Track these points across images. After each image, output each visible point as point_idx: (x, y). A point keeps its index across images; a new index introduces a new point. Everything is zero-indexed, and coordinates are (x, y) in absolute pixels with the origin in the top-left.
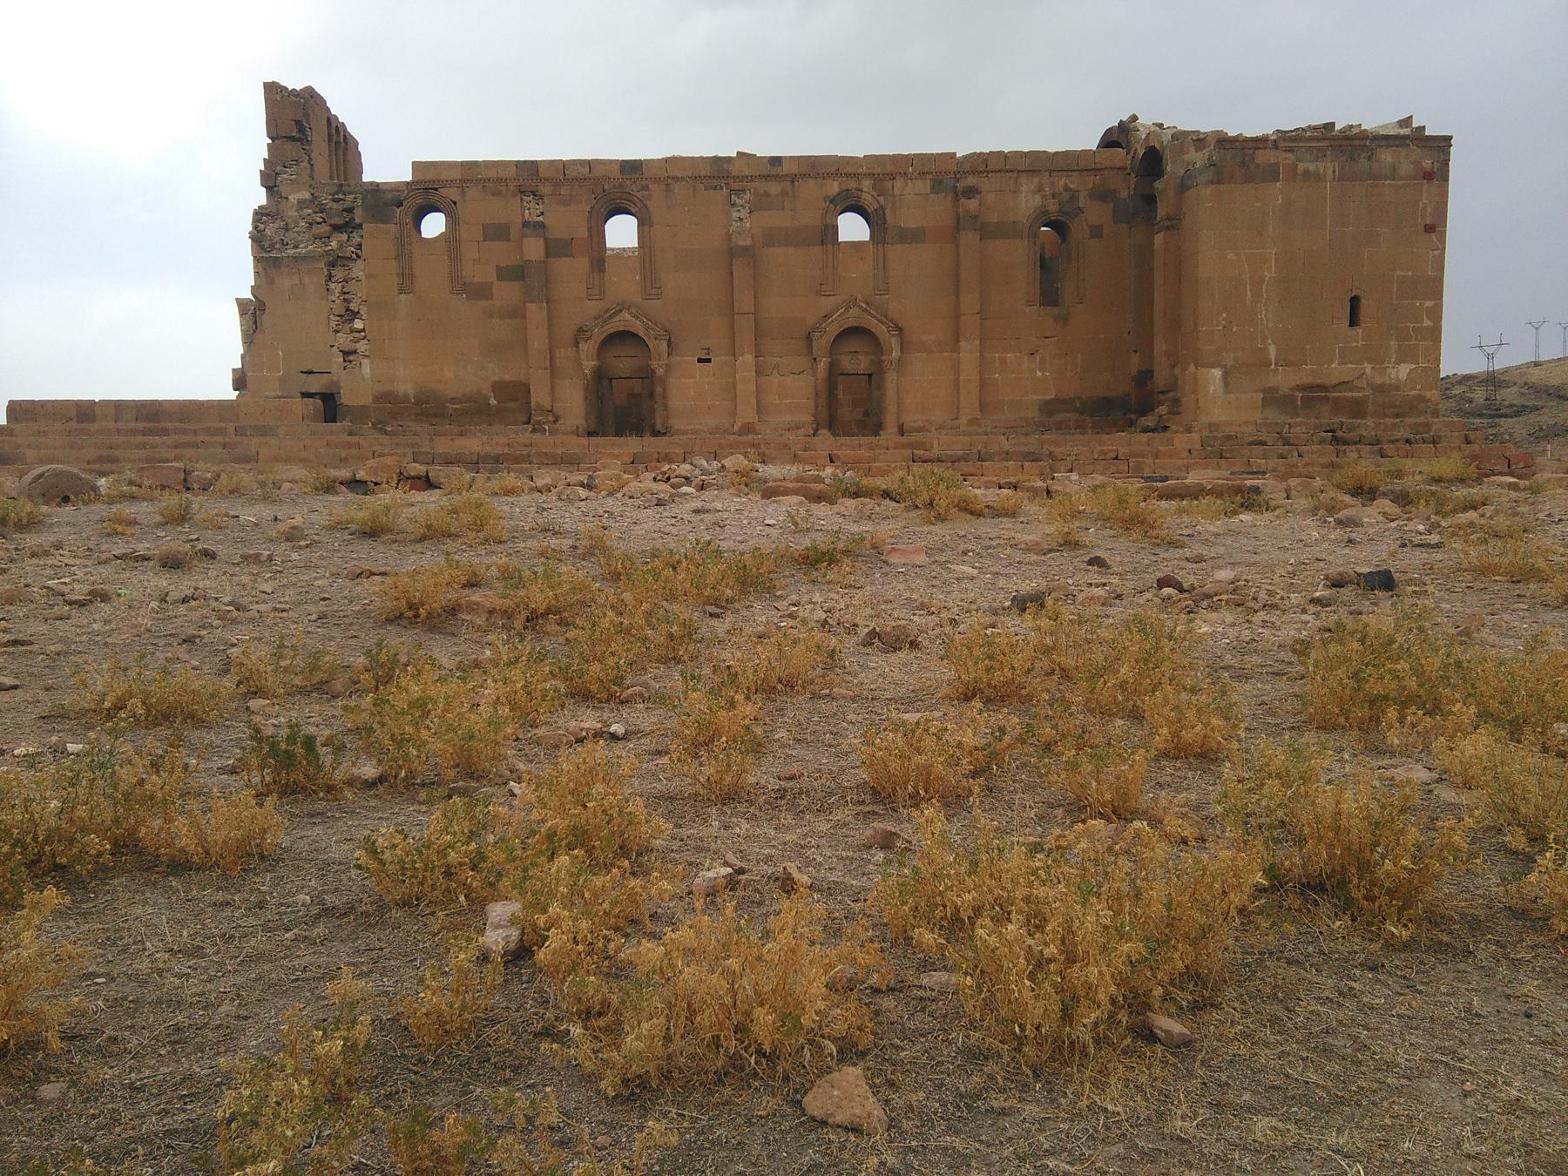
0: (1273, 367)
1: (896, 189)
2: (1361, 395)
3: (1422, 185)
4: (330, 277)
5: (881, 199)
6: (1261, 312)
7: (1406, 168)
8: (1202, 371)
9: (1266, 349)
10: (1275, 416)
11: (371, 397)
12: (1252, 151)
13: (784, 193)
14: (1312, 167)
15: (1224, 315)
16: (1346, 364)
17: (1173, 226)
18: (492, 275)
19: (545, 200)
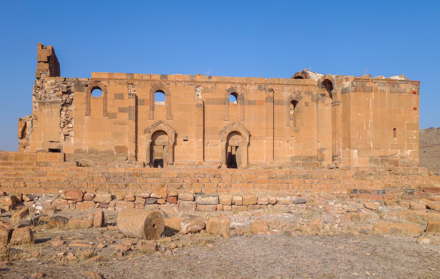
0: (372, 150)
1: (247, 88)
2: (397, 159)
3: (412, 95)
4: (61, 110)
5: (243, 91)
6: (368, 132)
7: (408, 90)
8: (351, 150)
9: (370, 144)
10: (373, 165)
11: (73, 151)
12: (365, 83)
13: (212, 87)
14: (382, 88)
15: (358, 133)
16: (393, 149)
17: (339, 104)
18: (116, 110)
19: (136, 86)
